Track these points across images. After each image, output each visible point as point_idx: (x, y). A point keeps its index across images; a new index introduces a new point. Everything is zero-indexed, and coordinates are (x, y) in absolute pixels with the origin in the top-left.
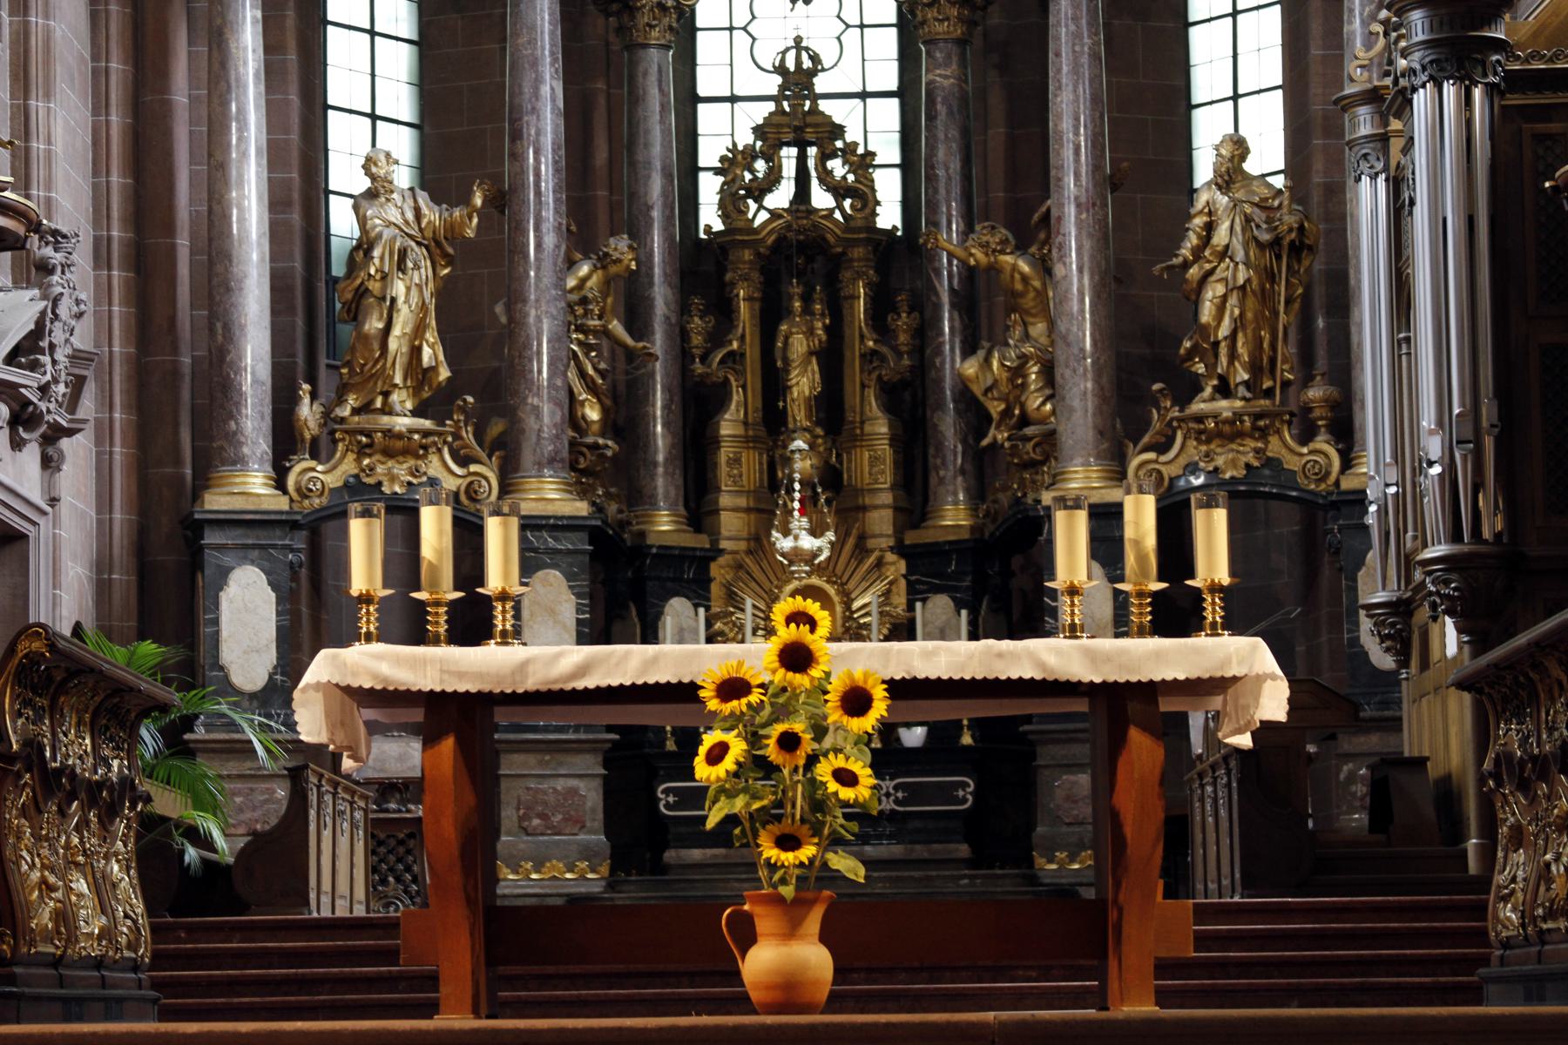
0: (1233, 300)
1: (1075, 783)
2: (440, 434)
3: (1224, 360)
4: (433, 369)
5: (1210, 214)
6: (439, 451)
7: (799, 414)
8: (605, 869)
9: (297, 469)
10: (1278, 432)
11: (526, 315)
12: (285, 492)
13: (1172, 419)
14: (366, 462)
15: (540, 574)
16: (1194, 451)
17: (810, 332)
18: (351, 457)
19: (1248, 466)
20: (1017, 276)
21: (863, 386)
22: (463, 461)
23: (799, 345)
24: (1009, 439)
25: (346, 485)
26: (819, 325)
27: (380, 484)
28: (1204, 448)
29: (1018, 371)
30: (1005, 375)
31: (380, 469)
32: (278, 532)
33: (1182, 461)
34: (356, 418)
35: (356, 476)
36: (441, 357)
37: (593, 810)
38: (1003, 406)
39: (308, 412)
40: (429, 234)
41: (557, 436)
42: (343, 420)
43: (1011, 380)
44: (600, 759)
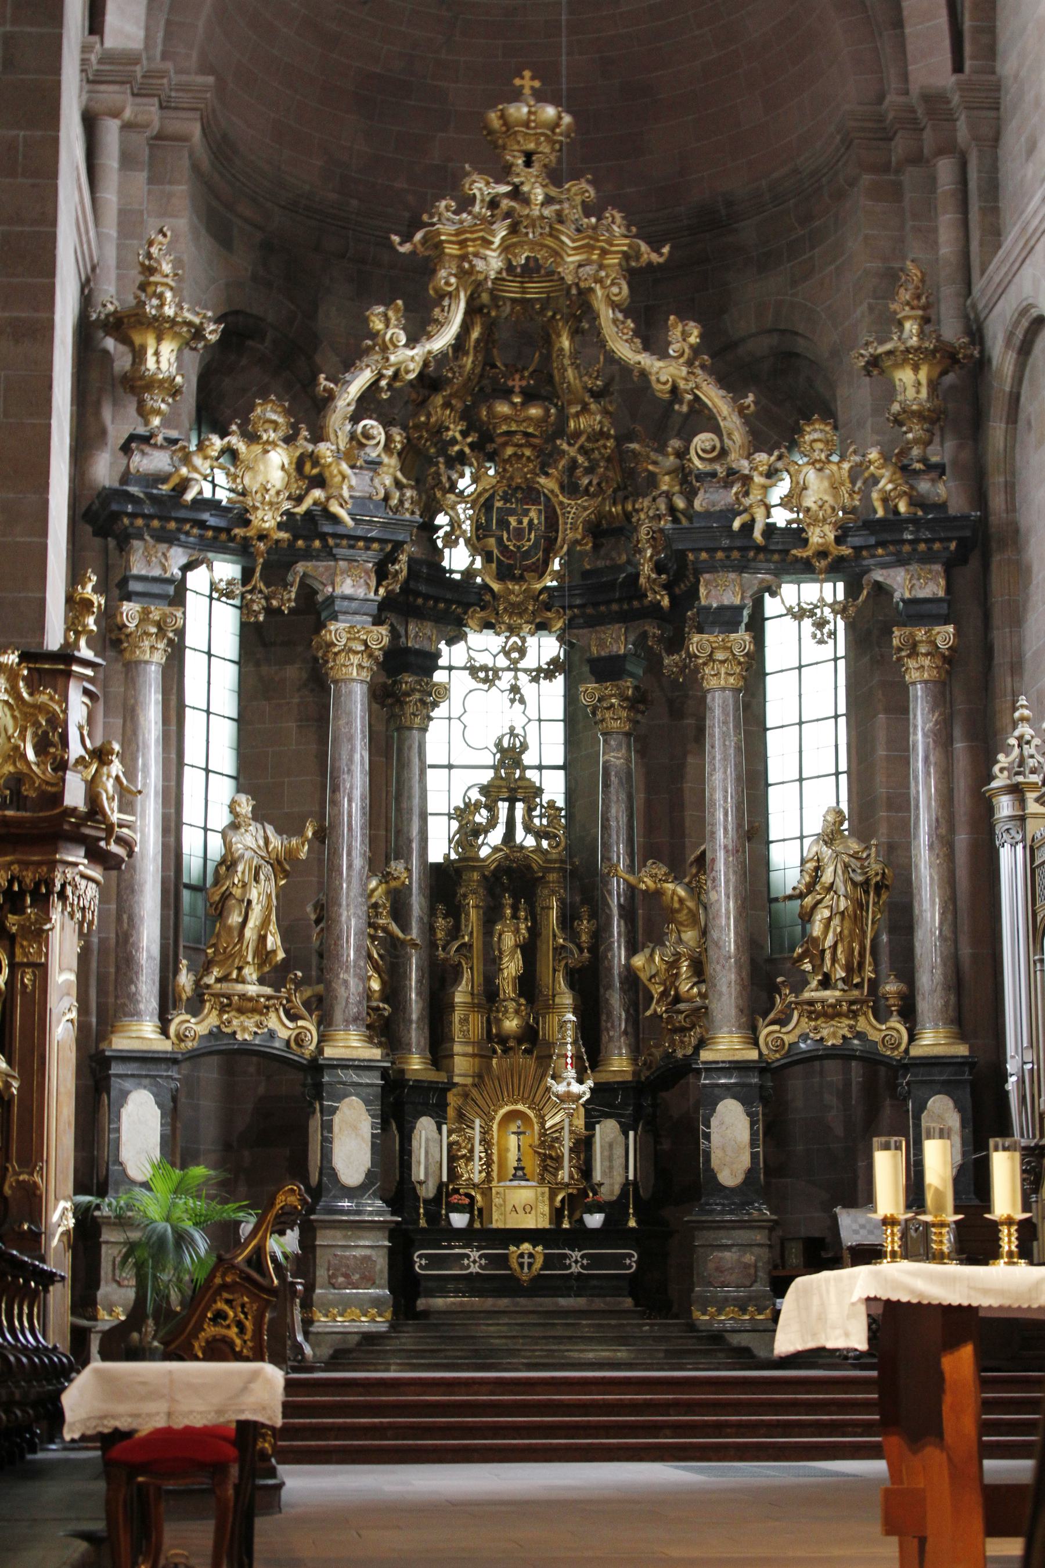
0: (836, 921)
1: (721, 1258)
2: (278, 998)
3: (828, 962)
4: (274, 952)
5: (818, 860)
6: (277, 1010)
7: (507, 988)
8: (388, 1315)
9: (177, 1020)
10: (865, 1014)
11: (340, 915)
12: (168, 1037)
13: (791, 1003)
14: (225, 1016)
15: (347, 1100)
16: (806, 1025)
17: (517, 931)
18: (215, 1013)
19: (844, 1037)
20: (676, 898)
21: (554, 970)
22: (293, 1017)
23: (509, 940)
24: (666, 1011)
25: (211, 1033)
26: (523, 926)
27: (235, 1033)
28: (813, 1023)
29: (674, 964)
30: (664, 966)
31: (235, 1022)
32: (163, 1066)
33: (797, 1032)
34: (219, 985)
35: (218, 1027)
36: (279, 943)
37: (381, 1271)
38: (662, 989)
39: (185, 980)
40: (273, 855)
41: (360, 1002)
42: (208, 986)
43: (667, 970)
44: (387, 1234)
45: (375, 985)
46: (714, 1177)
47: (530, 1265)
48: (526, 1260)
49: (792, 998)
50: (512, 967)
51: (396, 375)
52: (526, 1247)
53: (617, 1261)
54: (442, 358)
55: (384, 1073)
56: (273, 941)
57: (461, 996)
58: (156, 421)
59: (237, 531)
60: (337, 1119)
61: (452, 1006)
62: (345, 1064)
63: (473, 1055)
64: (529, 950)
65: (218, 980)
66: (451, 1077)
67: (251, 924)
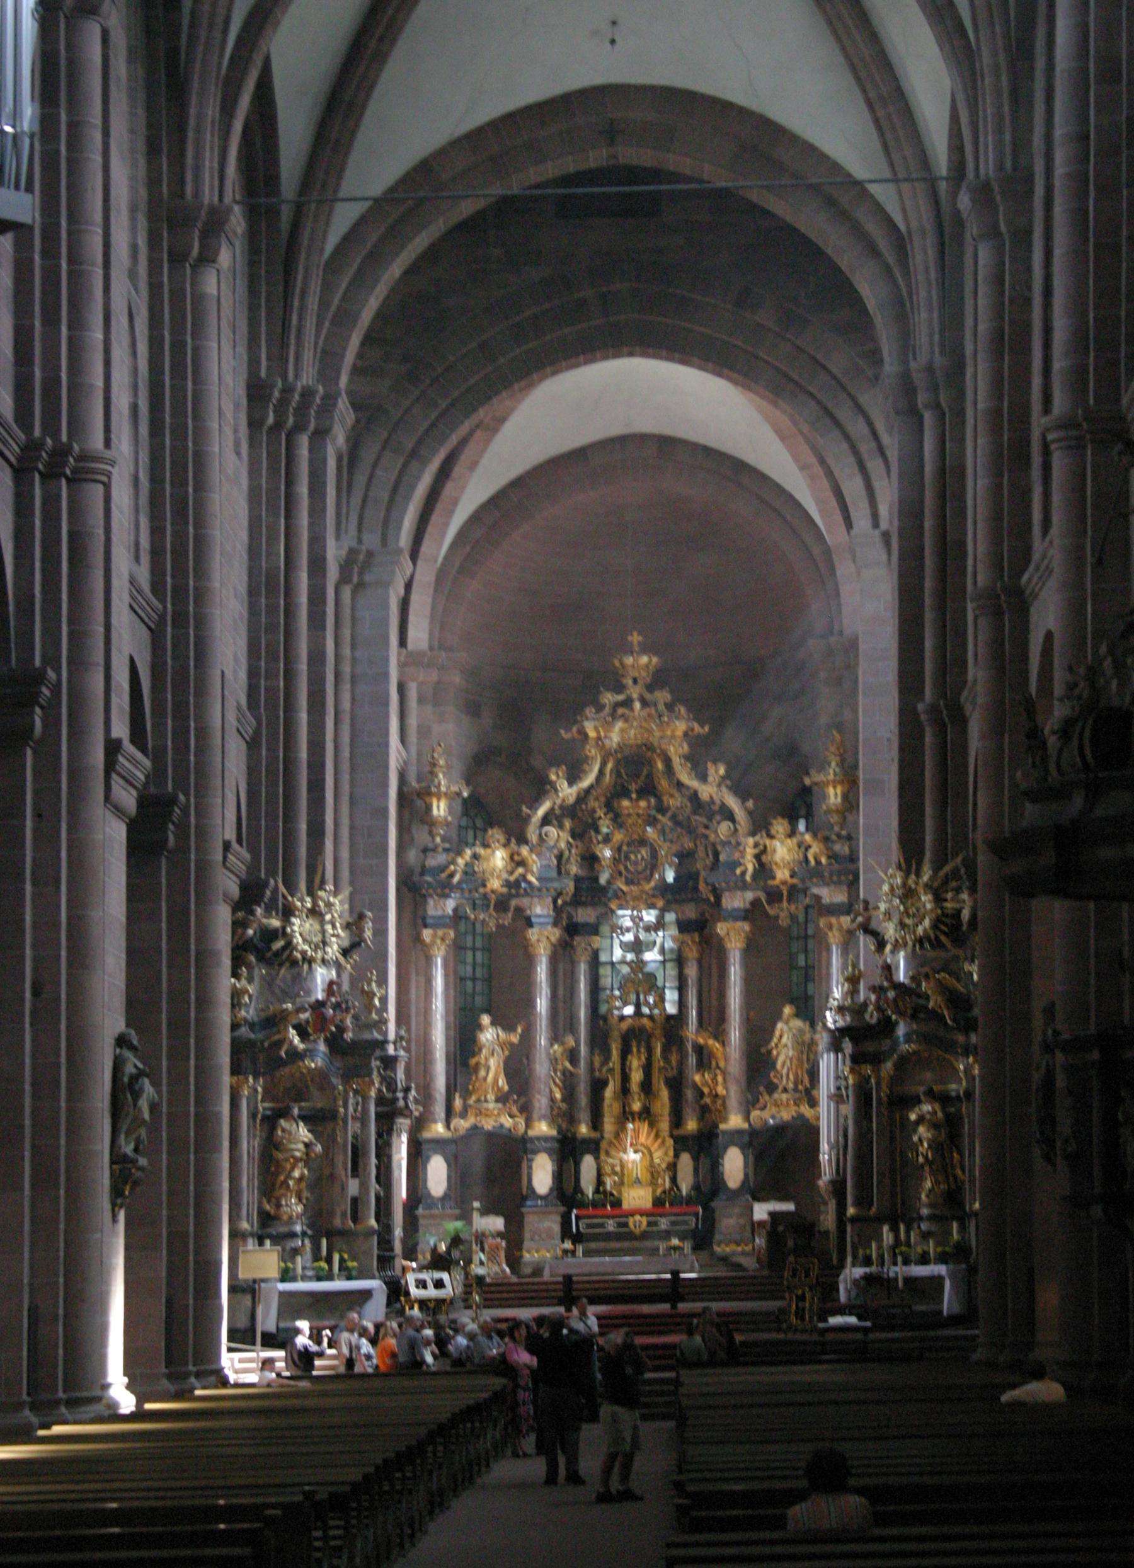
7: (634, 1086)
17: (639, 1059)
22: (512, 1116)
45: (558, 1096)
50: (636, 1076)
54: (591, 787)
56: (502, 1082)
57: (609, 1092)
61: (603, 1099)
64: (647, 1069)
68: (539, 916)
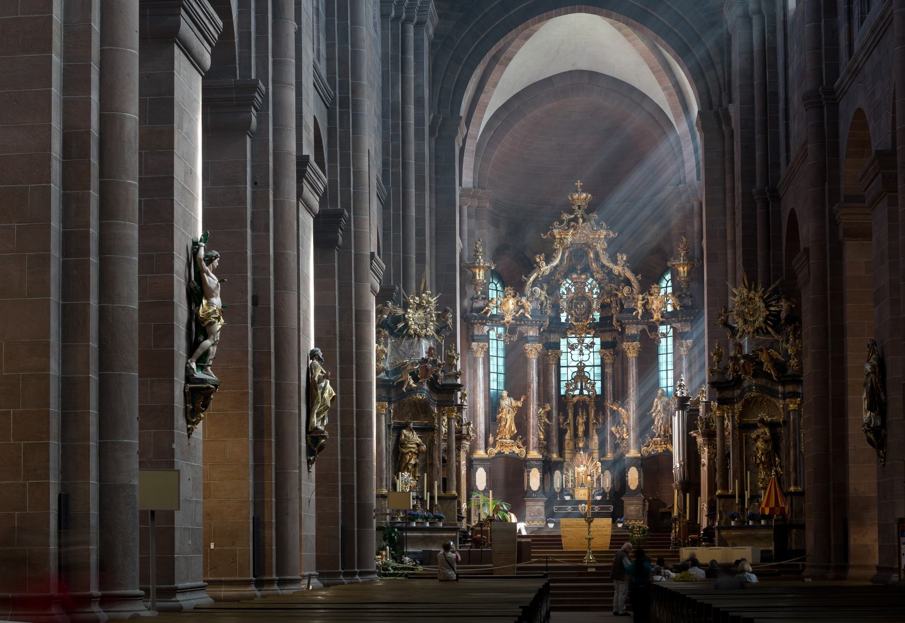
7: (580, 433)
12: (487, 454)
17: (583, 419)
22: (519, 447)
23: (581, 421)
29: (622, 429)
33: (651, 449)
39: (491, 439)
42: (497, 441)
44: (544, 503)
45: (542, 437)
46: (629, 487)
47: (584, 510)
48: (583, 508)
49: (650, 440)
50: (581, 429)
51: (543, 273)
52: (583, 505)
53: (608, 508)
54: (557, 266)
55: (543, 462)
56: (513, 428)
57: (567, 437)
58: (479, 293)
59: (502, 321)
60: (531, 474)
61: (565, 440)
62: (533, 460)
63: (570, 453)
64: (587, 424)
65: (500, 439)
66: (564, 460)
67: (508, 424)
68: (532, 336)
